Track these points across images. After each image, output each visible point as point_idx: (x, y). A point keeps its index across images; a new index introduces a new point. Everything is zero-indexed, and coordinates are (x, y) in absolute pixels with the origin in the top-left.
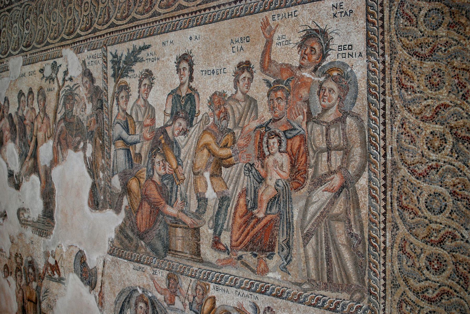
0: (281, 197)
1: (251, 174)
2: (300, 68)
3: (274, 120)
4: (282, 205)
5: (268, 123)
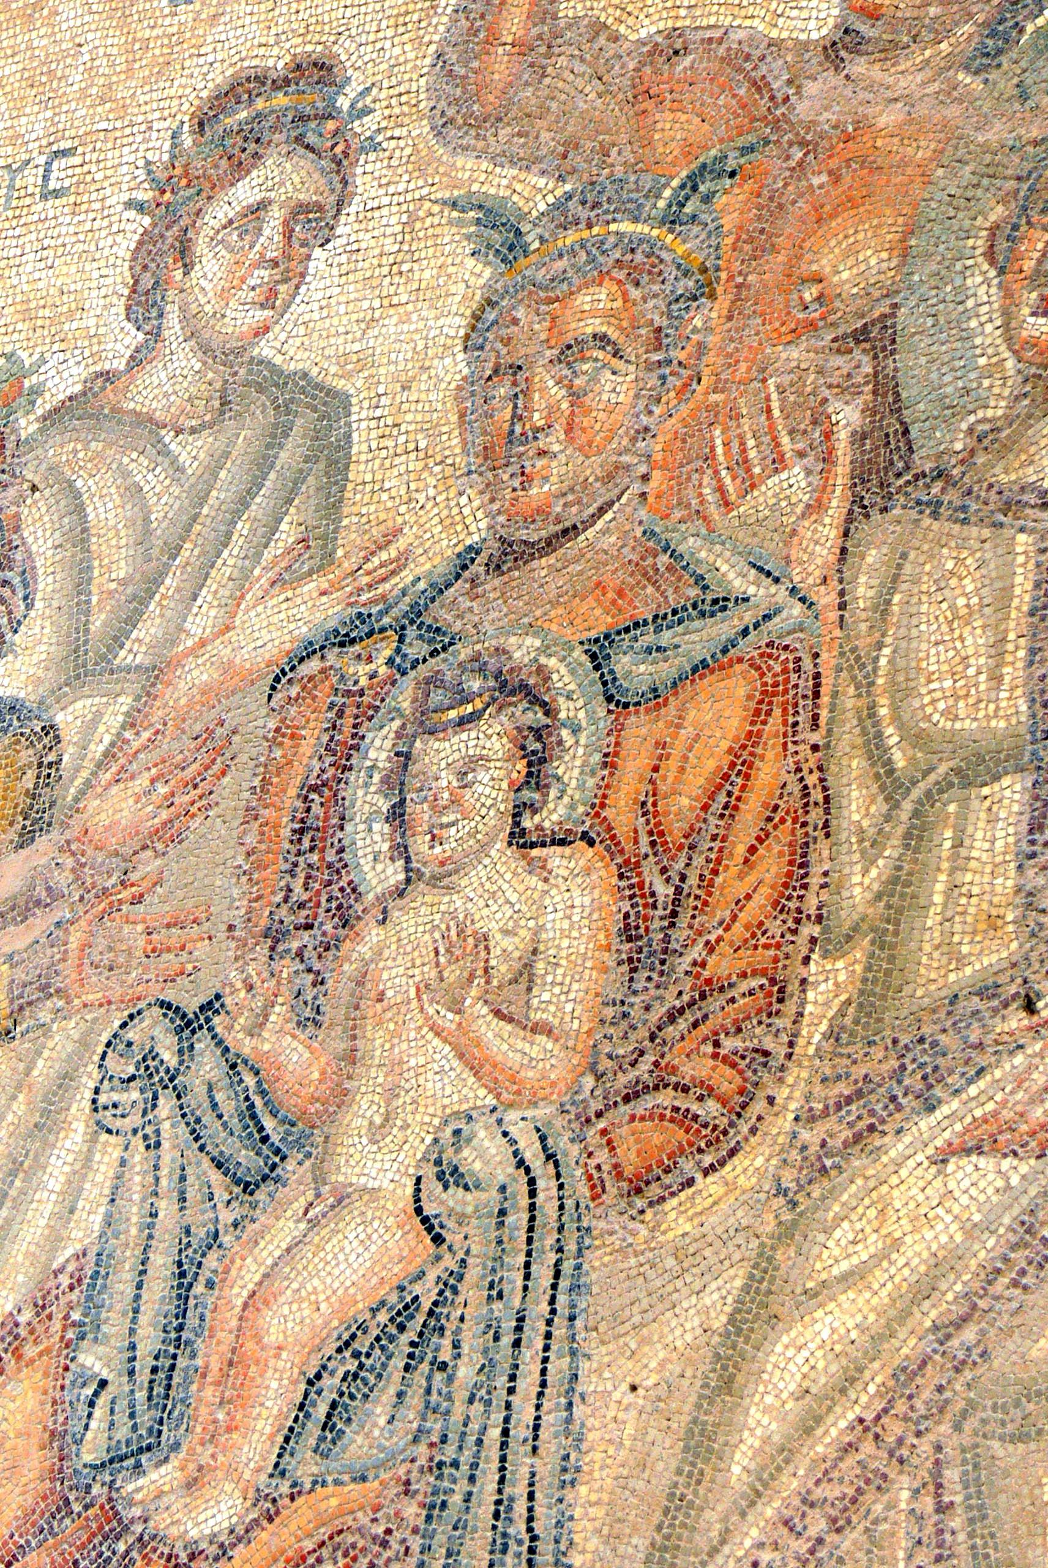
0: (471, 1292)
1: (166, 1105)
2: (841, 47)
3: (509, 555)
4: (465, 1372)
5: (439, 590)
